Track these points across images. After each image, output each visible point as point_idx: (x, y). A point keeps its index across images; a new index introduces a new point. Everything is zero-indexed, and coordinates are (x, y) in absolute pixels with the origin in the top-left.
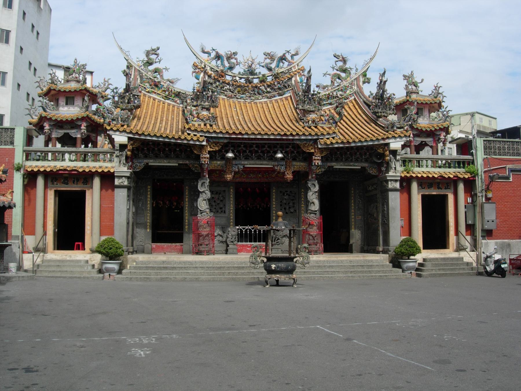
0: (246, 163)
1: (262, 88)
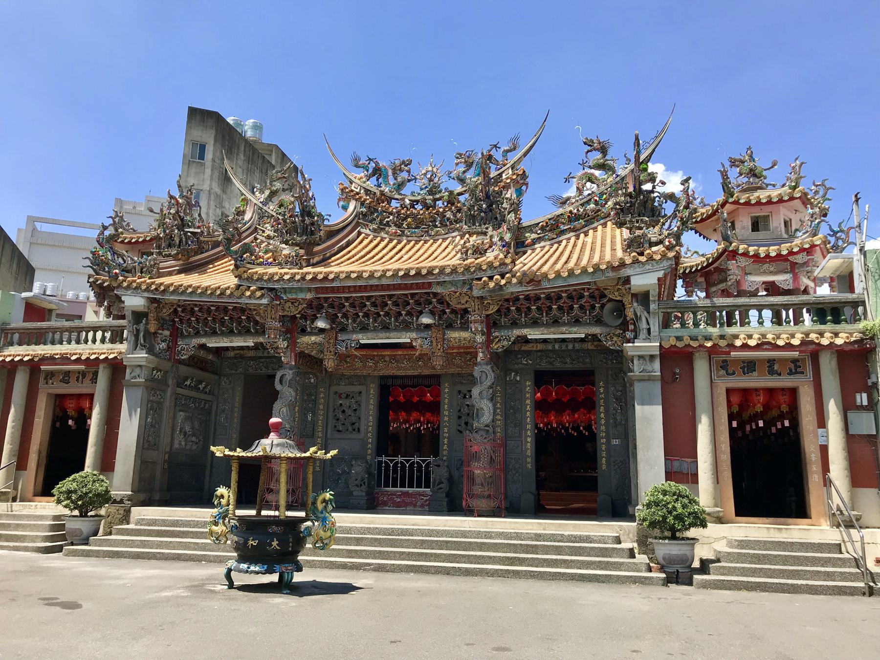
0: (360, 336)
1: (449, 214)
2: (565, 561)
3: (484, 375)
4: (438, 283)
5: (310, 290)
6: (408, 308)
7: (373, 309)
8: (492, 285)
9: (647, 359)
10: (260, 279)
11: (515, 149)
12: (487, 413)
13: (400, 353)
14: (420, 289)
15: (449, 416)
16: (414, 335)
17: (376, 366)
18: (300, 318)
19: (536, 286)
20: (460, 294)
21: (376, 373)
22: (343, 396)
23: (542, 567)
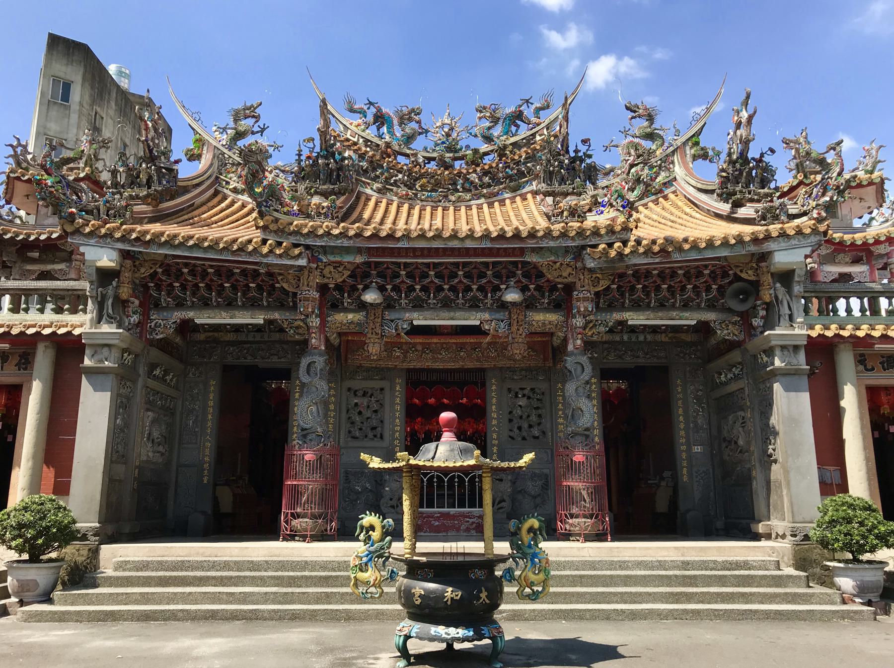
0: (415, 315)
1: (473, 177)
2: (743, 595)
3: (579, 368)
4: (533, 250)
5: (359, 251)
6: (484, 281)
7: (436, 281)
8: (613, 253)
9: (791, 350)
10: (297, 233)
11: (548, 107)
12: (587, 415)
13: (435, 340)
14: (509, 256)
15: (498, 419)
16: (487, 316)
17: (405, 357)
18: (334, 289)
19: (665, 257)
20: (561, 264)
21: (405, 365)
22: (360, 393)
23: (716, 602)
